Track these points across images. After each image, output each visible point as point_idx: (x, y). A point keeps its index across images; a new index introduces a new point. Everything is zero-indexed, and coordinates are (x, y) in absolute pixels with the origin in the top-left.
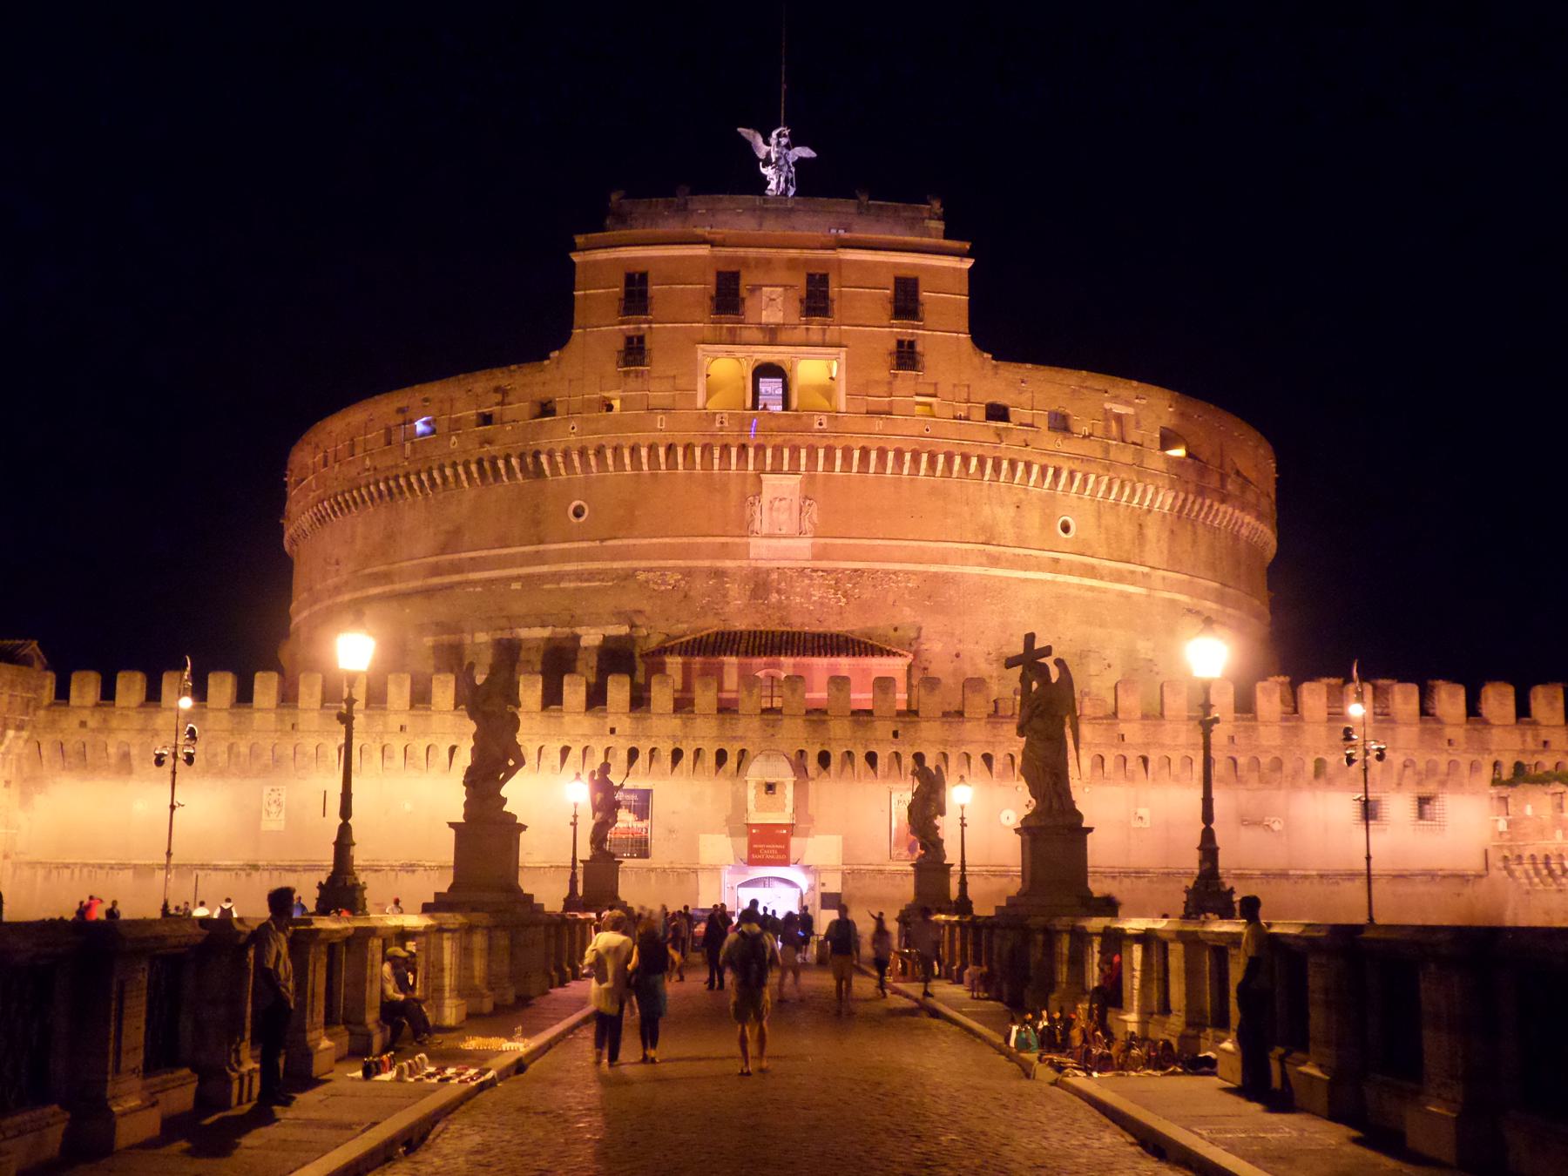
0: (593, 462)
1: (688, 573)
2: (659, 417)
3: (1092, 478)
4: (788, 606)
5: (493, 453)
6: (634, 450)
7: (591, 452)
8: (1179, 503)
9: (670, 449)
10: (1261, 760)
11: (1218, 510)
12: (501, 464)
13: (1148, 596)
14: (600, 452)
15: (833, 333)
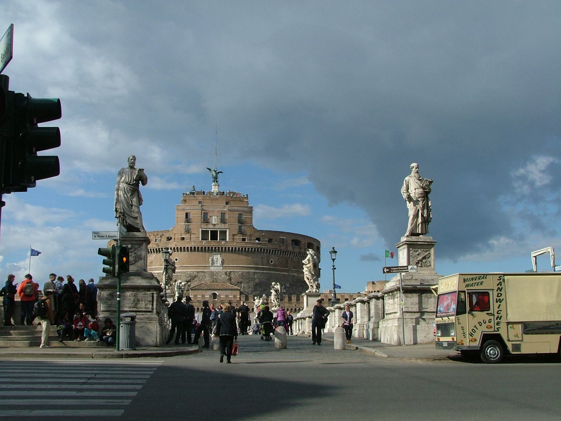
0: (179, 250)
1: (198, 272)
2: (192, 242)
3: (277, 252)
4: (218, 279)
5: (159, 248)
6: (188, 248)
7: (179, 248)
8: (295, 255)
9: (195, 248)
10: (301, 309)
11: (304, 256)
12: (161, 250)
13: (288, 274)
14: (181, 248)
15: (226, 226)
